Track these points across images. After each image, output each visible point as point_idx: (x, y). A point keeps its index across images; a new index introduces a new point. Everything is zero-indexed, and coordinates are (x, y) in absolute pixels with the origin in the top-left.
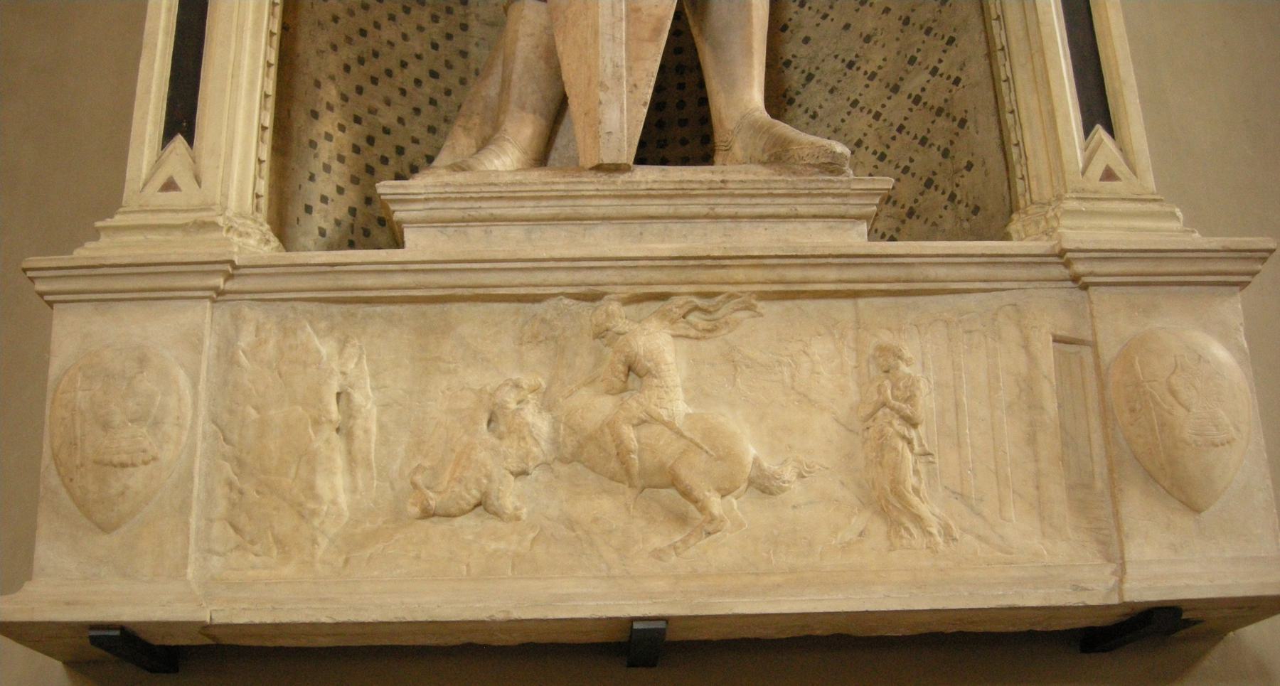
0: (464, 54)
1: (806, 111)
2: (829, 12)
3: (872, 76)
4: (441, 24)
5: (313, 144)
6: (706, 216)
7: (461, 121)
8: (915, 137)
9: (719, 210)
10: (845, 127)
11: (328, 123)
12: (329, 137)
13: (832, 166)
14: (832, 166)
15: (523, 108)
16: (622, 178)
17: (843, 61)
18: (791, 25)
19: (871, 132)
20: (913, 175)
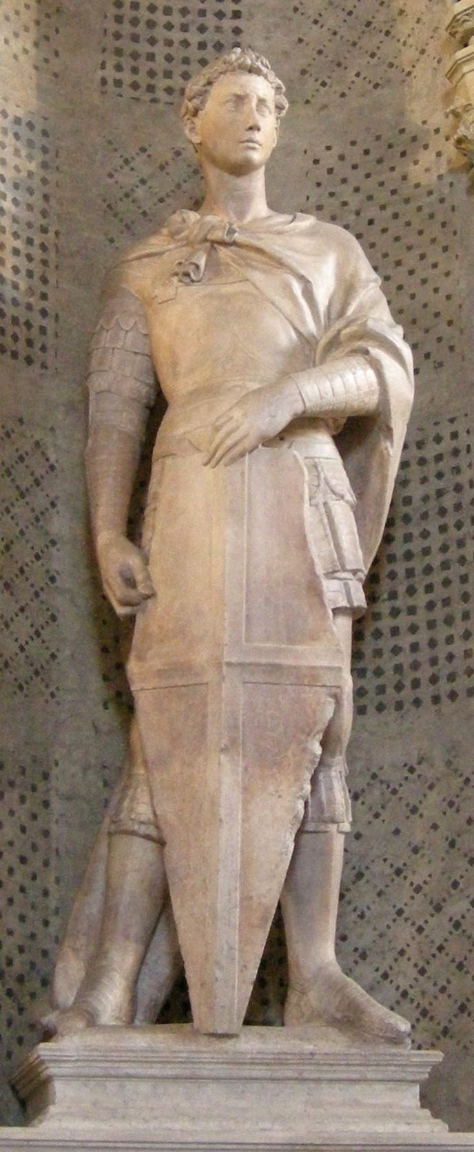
0: (46, 833)
1: (355, 910)
2: (381, 811)
3: (418, 889)
4: (27, 805)
6: (296, 1079)
7: (68, 942)
8: (453, 961)
9: (306, 1075)
10: (390, 933)
13: (395, 1039)
14: (395, 1039)
15: (127, 937)
16: (229, 1045)
17: (392, 866)
19: (413, 945)
20: (450, 996)
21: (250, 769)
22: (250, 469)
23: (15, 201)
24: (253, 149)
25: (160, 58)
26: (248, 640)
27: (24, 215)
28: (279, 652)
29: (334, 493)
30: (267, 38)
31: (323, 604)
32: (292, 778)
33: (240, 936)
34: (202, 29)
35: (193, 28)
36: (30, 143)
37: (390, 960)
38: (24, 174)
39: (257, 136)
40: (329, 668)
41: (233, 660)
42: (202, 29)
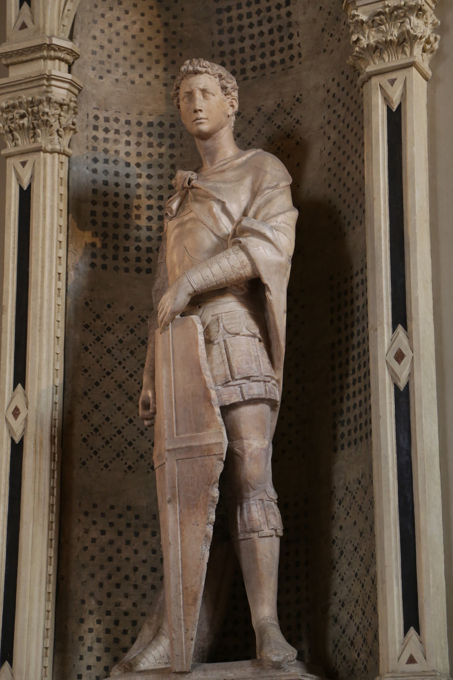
5: (81, 638)
11: (91, 622)
12: (91, 630)
18: (335, 515)
21: (183, 511)
22: (172, 332)
23: (149, 177)
24: (201, 123)
25: (247, 50)
26: (177, 435)
27: (155, 182)
28: (191, 438)
29: (229, 333)
30: (305, 13)
31: (211, 406)
32: (203, 513)
33: (184, 611)
34: (270, 20)
35: (265, 22)
36: (161, 136)
37: (353, 608)
38: (156, 157)
39: (201, 115)
40: (216, 444)
41: (170, 447)
42: (270, 20)
